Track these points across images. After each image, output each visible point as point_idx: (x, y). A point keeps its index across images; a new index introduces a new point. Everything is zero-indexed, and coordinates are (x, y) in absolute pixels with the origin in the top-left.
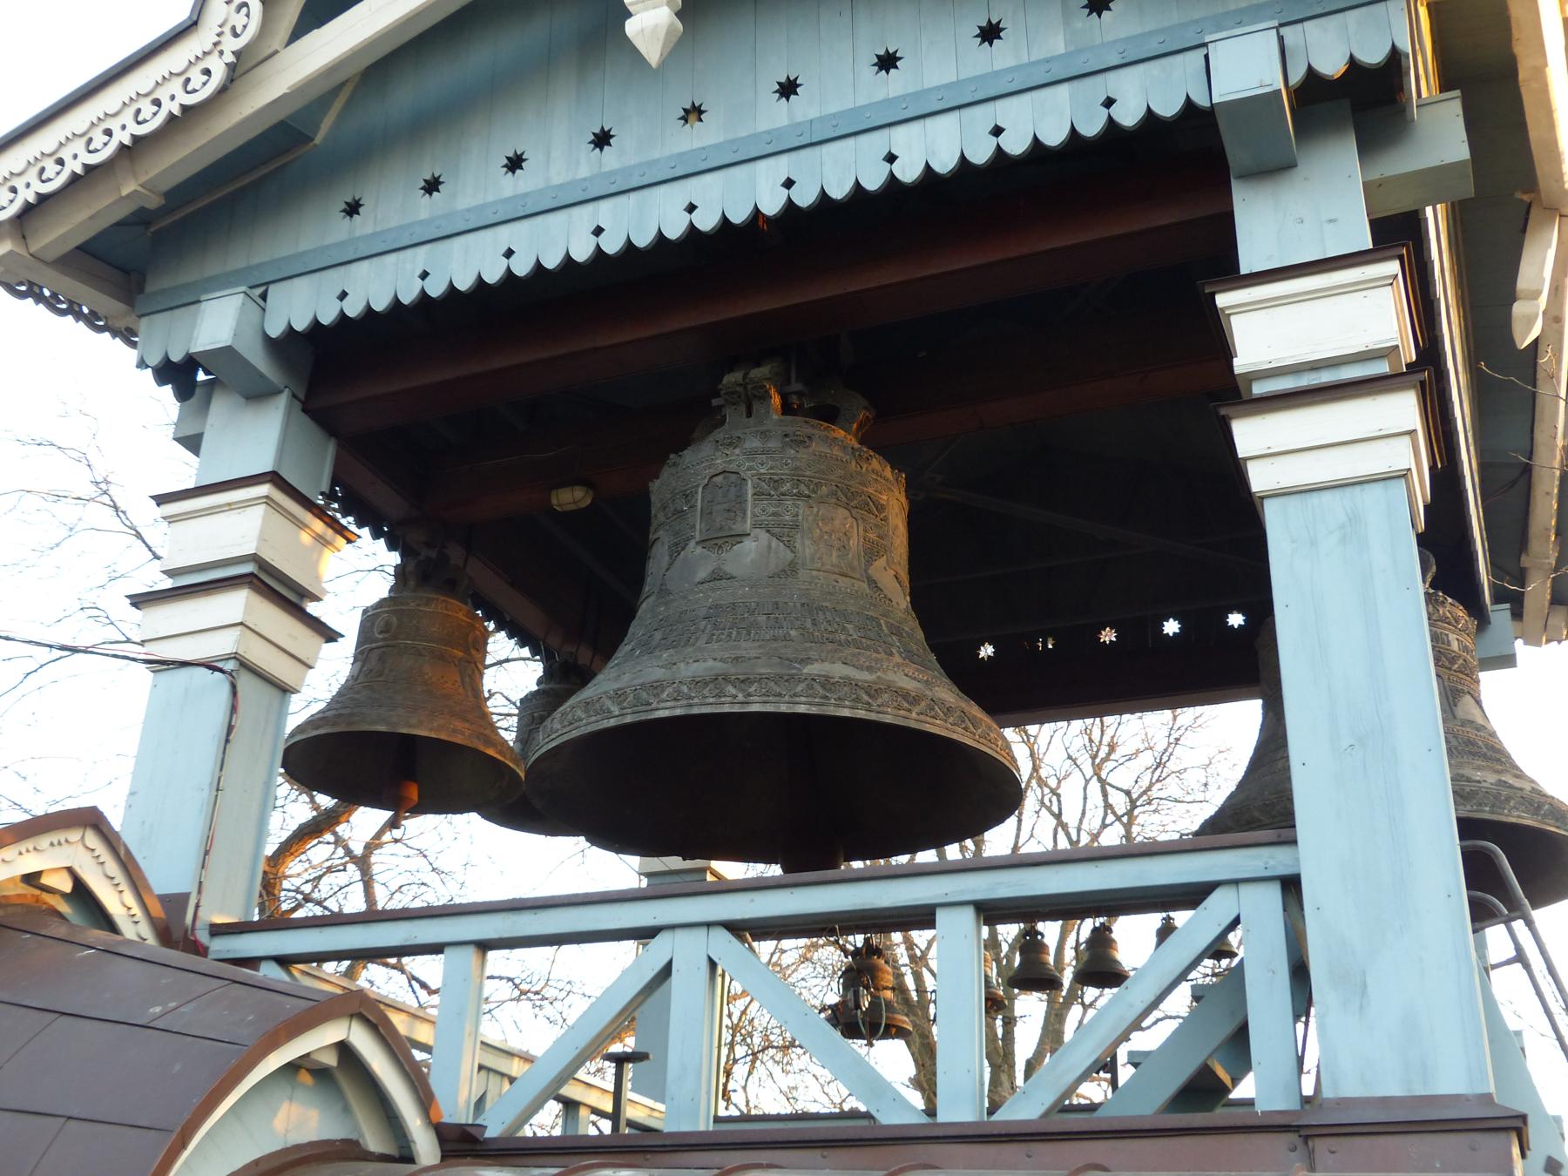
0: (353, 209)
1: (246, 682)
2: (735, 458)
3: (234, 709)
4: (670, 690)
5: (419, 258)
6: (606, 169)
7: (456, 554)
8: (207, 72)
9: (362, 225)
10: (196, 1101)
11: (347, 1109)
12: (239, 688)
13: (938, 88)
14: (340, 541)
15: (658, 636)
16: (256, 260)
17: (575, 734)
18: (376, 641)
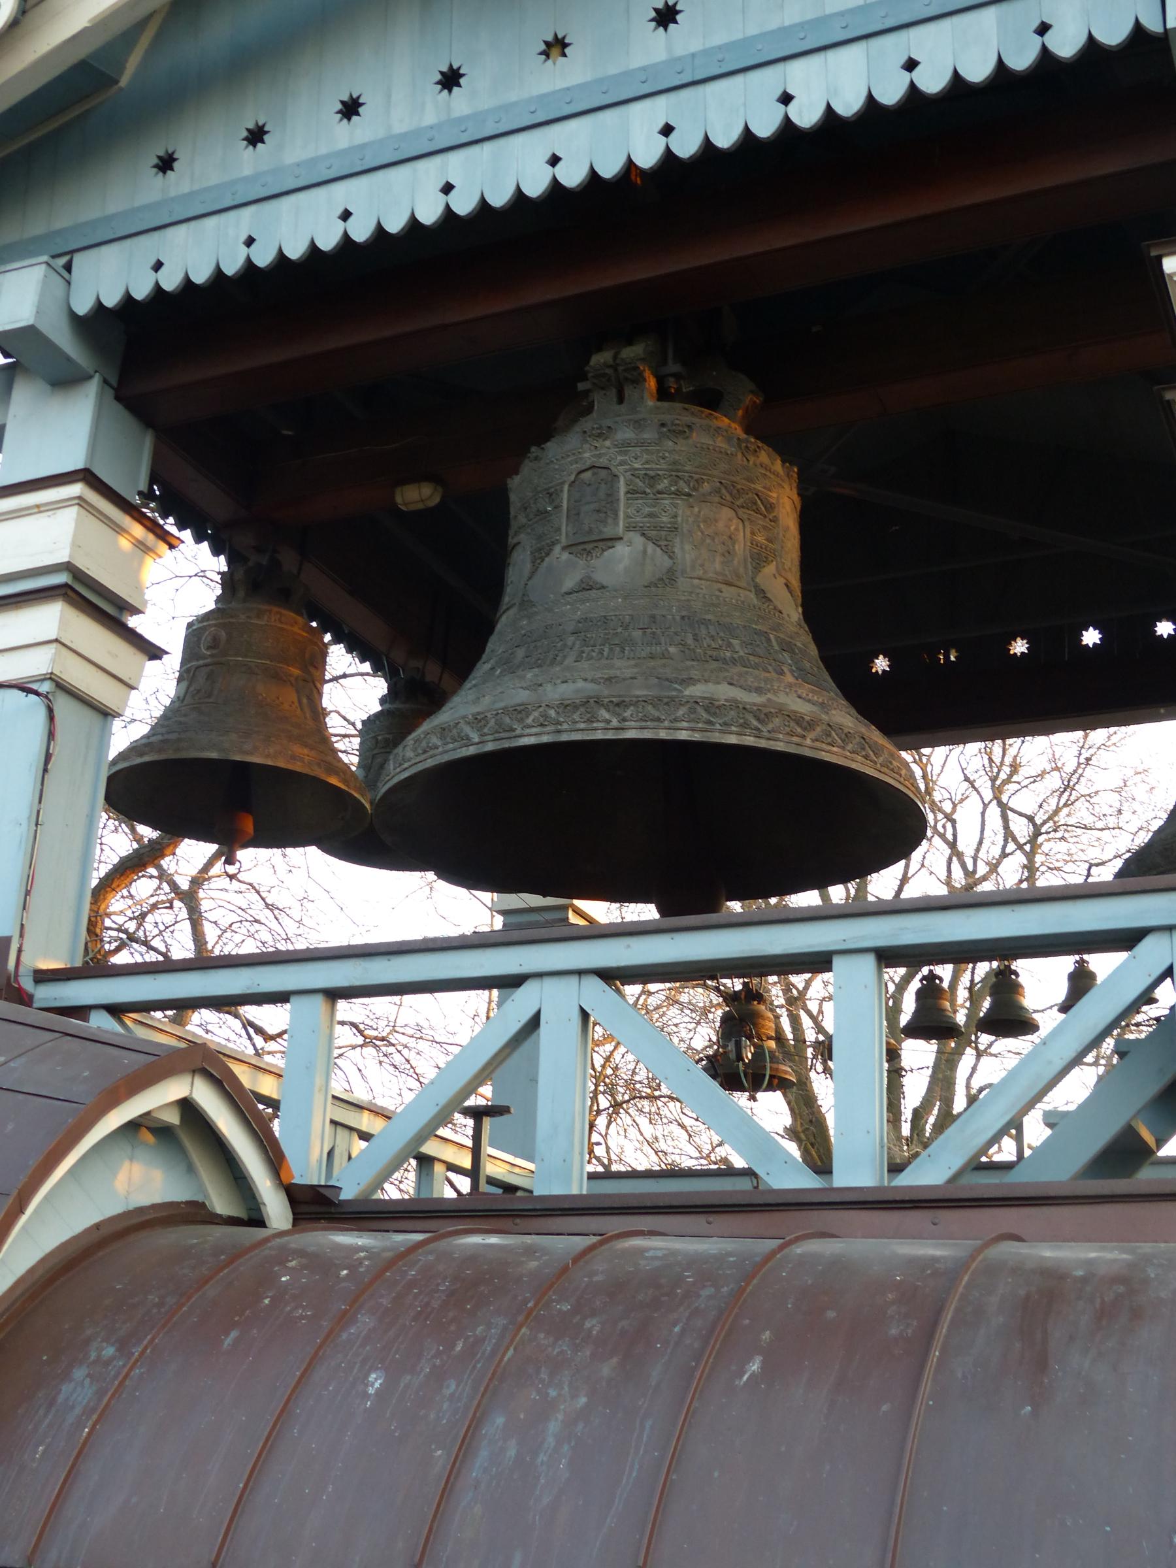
0: (166, 164)
1: (63, 705)
2: (605, 452)
3: (51, 735)
4: (536, 714)
5: (243, 222)
6: (456, 114)
7: (288, 559)
9: (178, 182)
10: (33, 1163)
11: (190, 1169)
12: (56, 713)
13: (842, 14)
14: (163, 547)
15: (520, 653)
16: (58, 225)
17: (430, 763)
18: (204, 657)
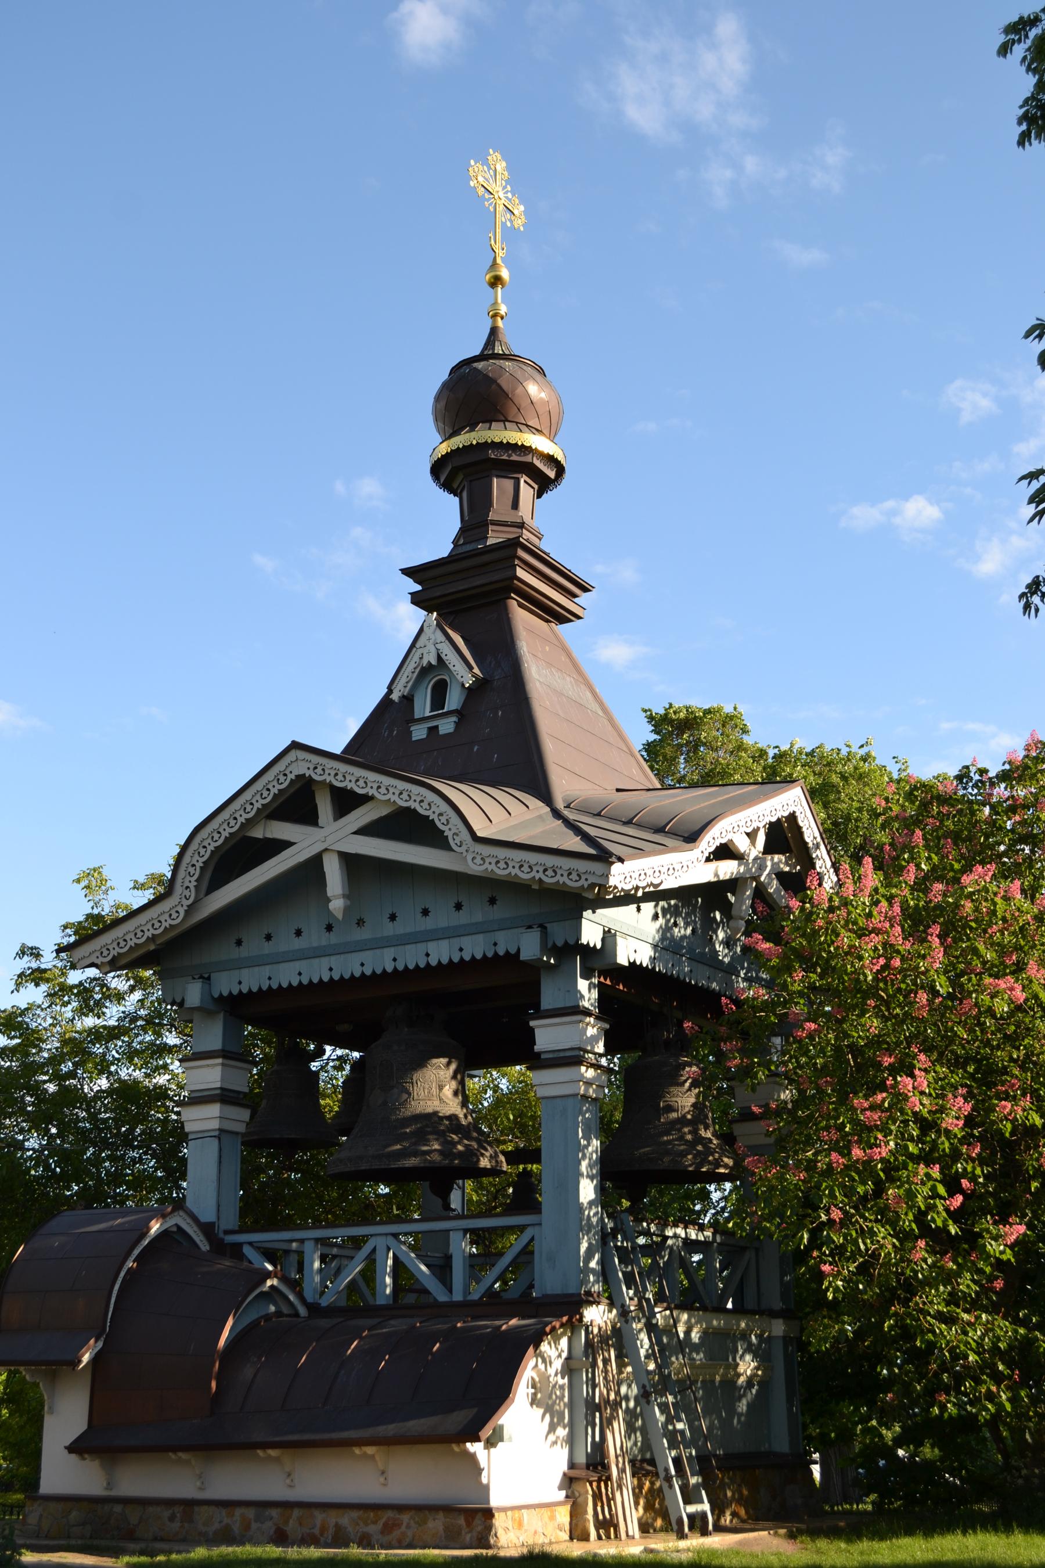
0: (239, 943)
5: (266, 971)
8: (177, 912)
9: (244, 951)
